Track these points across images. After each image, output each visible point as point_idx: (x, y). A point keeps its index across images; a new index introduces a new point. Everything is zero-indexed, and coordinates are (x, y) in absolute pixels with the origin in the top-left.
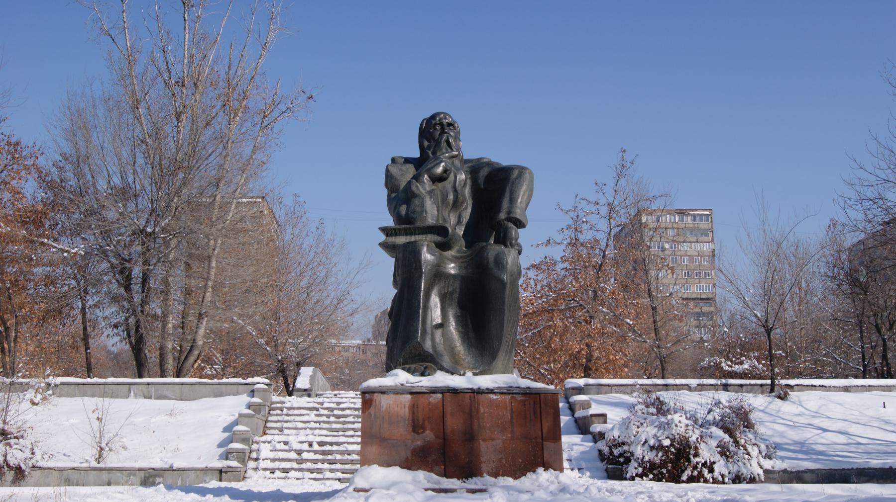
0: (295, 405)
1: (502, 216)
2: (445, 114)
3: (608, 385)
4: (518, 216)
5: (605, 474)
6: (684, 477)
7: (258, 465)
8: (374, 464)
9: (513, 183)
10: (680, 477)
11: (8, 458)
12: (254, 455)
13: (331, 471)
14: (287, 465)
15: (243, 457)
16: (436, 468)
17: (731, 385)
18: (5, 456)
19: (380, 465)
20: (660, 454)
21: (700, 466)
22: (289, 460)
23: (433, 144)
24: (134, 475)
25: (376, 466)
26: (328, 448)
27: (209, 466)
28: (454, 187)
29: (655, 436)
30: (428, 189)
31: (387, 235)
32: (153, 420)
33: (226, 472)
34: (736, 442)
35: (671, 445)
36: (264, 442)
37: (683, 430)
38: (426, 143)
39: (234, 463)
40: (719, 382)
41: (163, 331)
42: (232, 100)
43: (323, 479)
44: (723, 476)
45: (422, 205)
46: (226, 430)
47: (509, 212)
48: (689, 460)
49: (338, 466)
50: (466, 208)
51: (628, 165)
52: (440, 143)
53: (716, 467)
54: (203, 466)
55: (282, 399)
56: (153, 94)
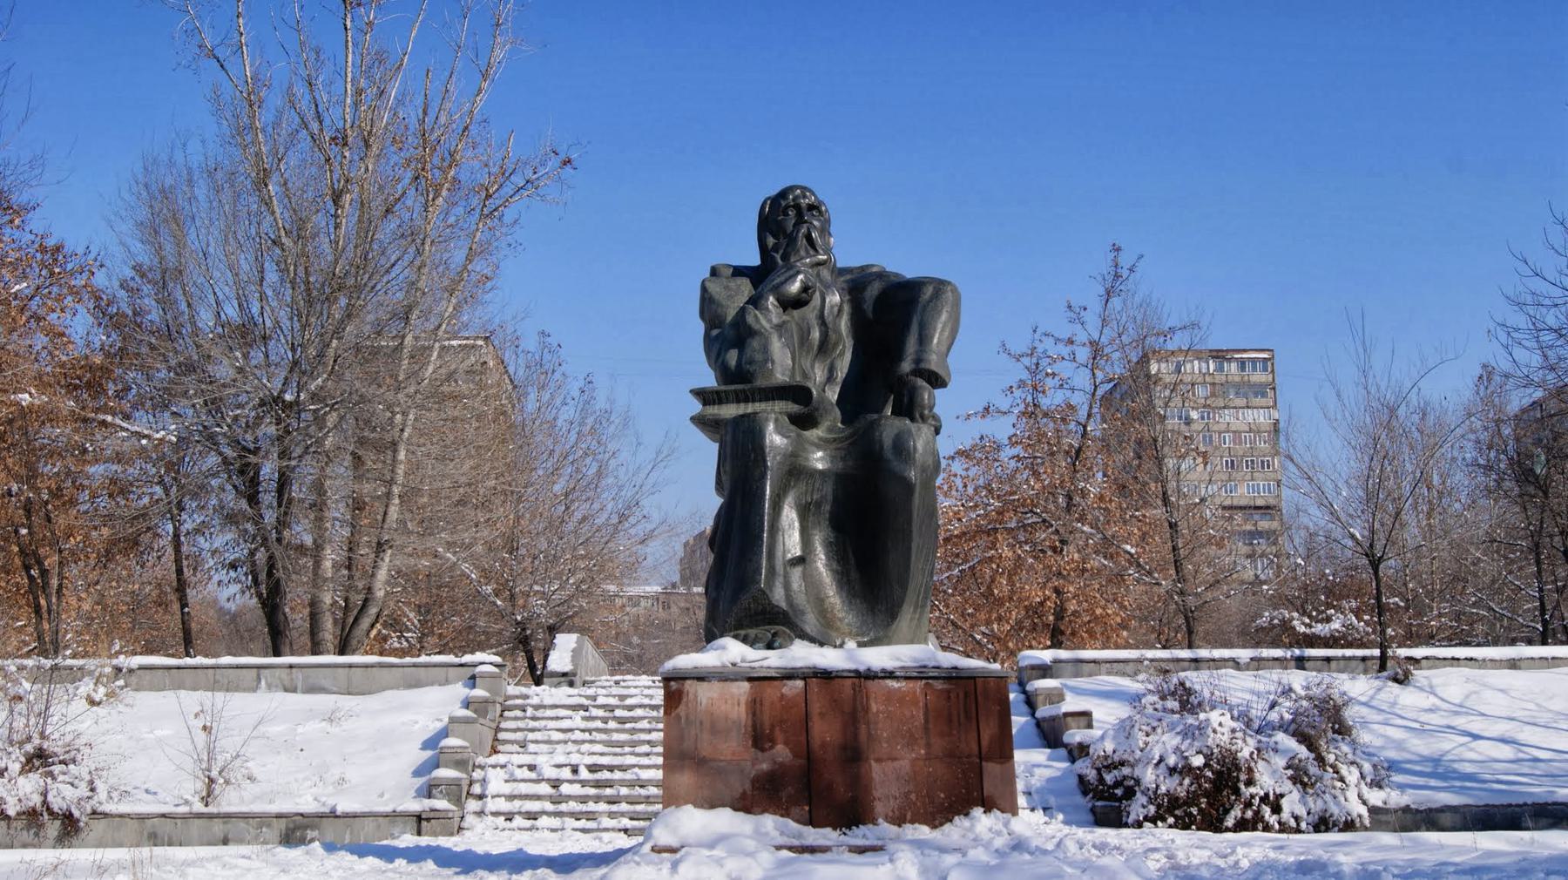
0: (547, 701)
1: (906, 366)
2: (804, 189)
3: (1094, 661)
4: (933, 367)
5: (1091, 818)
6: (1230, 822)
7: (485, 805)
8: (686, 803)
9: (925, 307)
10: (1222, 821)
11: (50, 798)
12: (477, 789)
13: (612, 815)
14: (534, 806)
15: (458, 794)
16: (795, 810)
17: (1310, 659)
18: (45, 794)
19: (696, 805)
20: (1187, 781)
21: (1256, 801)
22: (538, 797)
23: (784, 242)
24: (269, 826)
25: (690, 807)
26: (606, 775)
27: (400, 809)
28: (821, 317)
29: (1177, 750)
30: (775, 320)
31: (705, 403)
32: (300, 730)
33: (428, 820)
34: (1320, 760)
35: (1206, 765)
36: (494, 767)
37: (1226, 738)
38: (771, 241)
39: (441, 804)
40: (1289, 654)
41: (315, 573)
42: (431, 167)
43: (598, 830)
44: (1297, 818)
45: (765, 349)
46: (430, 744)
47: (918, 361)
48: (1237, 792)
49: (624, 807)
50: (842, 354)
51: (1125, 273)
52: (795, 239)
53: (1284, 802)
54: (388, 809)
55: (524, 690)
56: (293, 159)
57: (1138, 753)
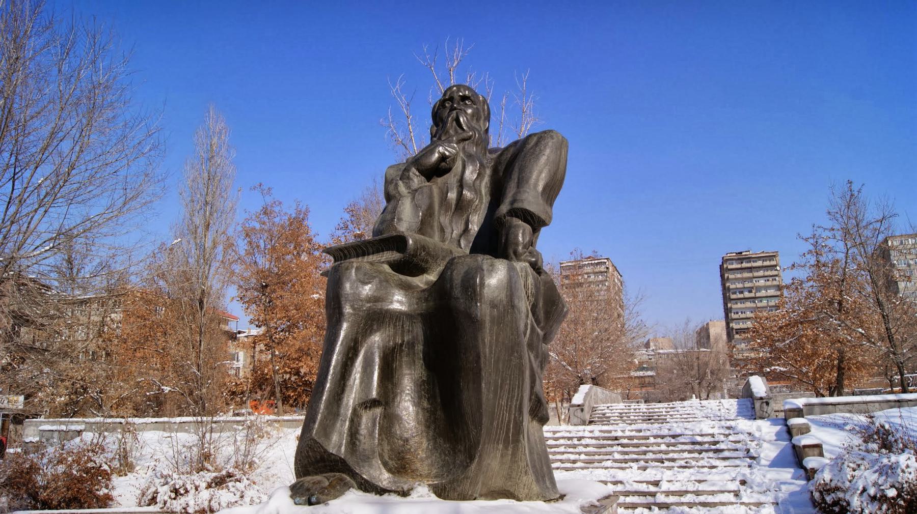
3: (831, 404)
20: (885, 507)
29: (875, 484)
35: (899, 495)
47: (514, 201)
51: (856, 194)
57: (848, 484)
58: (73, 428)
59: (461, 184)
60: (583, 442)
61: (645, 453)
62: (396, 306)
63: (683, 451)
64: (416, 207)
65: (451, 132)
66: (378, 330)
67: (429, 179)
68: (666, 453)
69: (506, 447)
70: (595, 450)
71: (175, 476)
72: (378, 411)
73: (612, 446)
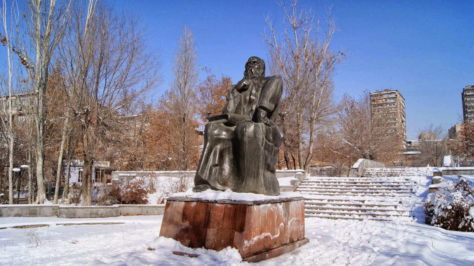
0: (312, 181)
5: (425, 220)
6: (460, 226)
10: (458, 225)
19: (165, 236)
20: (447, 213)
21: (469, 221)
31: (209, 121)
35: (453, 209)
48: (463, 217)
58: (132, 175)
59: (251, 94)
60: (341, 184)
61: (366, 189)
62: (223, 137)
63: (383, 189)
64: (235, 103)
65: (249, 75)
66: (218, 144)
67: (241, 92)
68: (375, 189)
69: (254, 178)
70: (345, 187)
71: (171, 193)
72: (218, 167)
73: (352, 186)
